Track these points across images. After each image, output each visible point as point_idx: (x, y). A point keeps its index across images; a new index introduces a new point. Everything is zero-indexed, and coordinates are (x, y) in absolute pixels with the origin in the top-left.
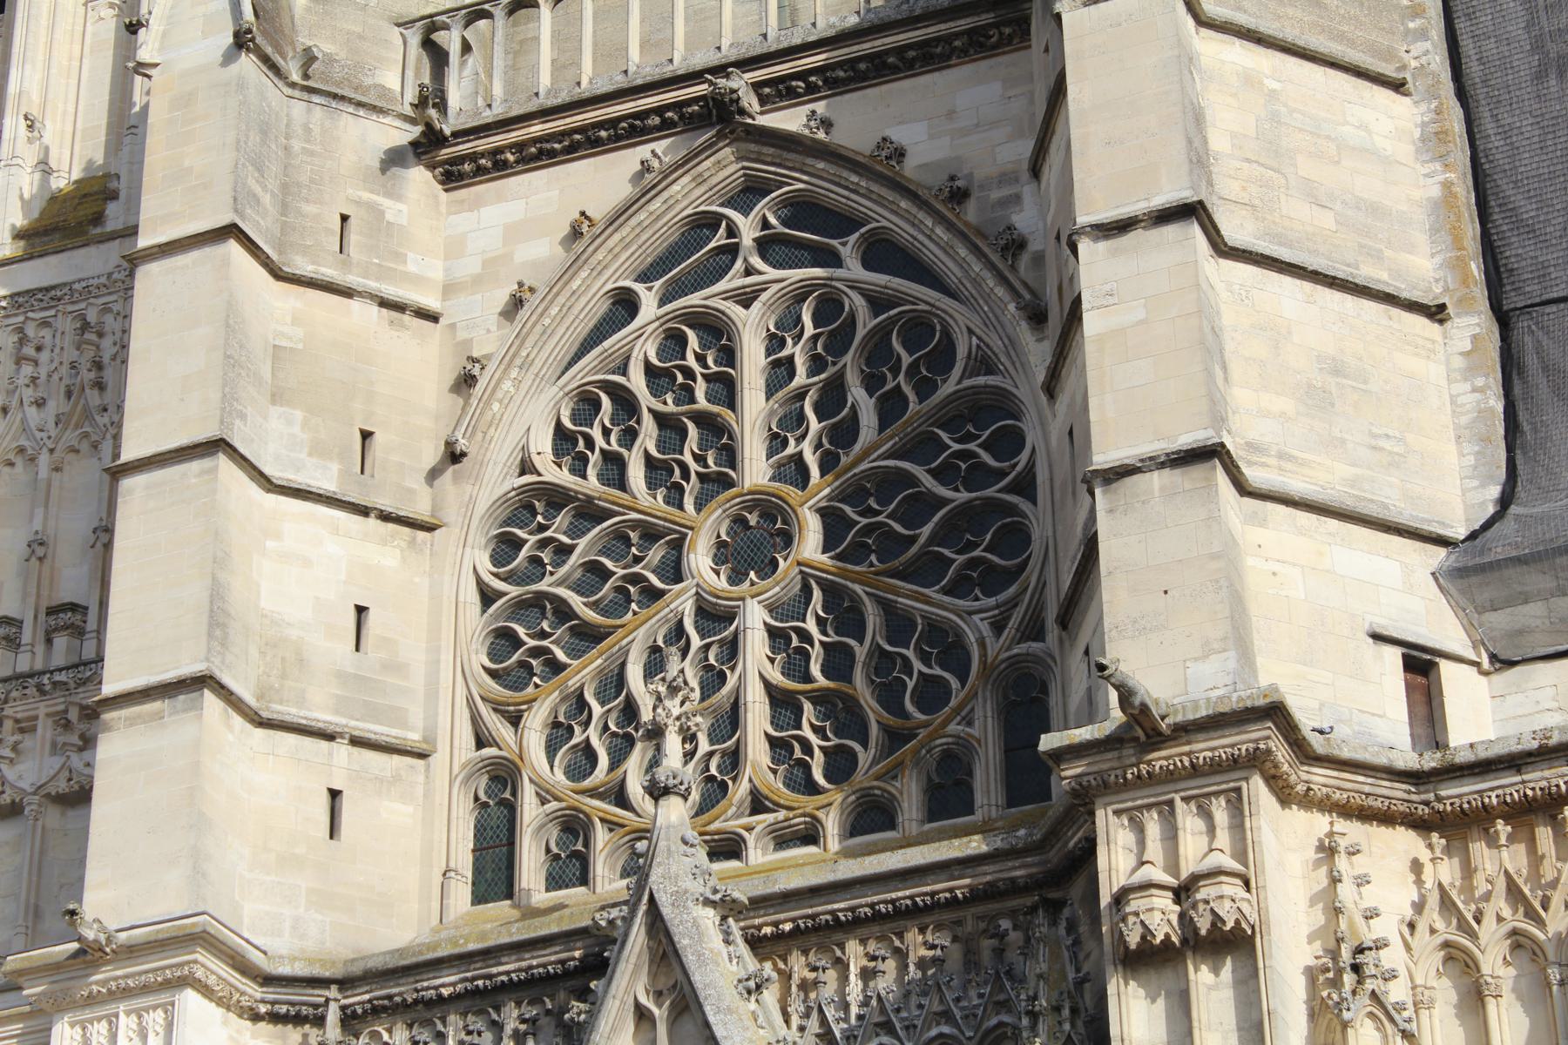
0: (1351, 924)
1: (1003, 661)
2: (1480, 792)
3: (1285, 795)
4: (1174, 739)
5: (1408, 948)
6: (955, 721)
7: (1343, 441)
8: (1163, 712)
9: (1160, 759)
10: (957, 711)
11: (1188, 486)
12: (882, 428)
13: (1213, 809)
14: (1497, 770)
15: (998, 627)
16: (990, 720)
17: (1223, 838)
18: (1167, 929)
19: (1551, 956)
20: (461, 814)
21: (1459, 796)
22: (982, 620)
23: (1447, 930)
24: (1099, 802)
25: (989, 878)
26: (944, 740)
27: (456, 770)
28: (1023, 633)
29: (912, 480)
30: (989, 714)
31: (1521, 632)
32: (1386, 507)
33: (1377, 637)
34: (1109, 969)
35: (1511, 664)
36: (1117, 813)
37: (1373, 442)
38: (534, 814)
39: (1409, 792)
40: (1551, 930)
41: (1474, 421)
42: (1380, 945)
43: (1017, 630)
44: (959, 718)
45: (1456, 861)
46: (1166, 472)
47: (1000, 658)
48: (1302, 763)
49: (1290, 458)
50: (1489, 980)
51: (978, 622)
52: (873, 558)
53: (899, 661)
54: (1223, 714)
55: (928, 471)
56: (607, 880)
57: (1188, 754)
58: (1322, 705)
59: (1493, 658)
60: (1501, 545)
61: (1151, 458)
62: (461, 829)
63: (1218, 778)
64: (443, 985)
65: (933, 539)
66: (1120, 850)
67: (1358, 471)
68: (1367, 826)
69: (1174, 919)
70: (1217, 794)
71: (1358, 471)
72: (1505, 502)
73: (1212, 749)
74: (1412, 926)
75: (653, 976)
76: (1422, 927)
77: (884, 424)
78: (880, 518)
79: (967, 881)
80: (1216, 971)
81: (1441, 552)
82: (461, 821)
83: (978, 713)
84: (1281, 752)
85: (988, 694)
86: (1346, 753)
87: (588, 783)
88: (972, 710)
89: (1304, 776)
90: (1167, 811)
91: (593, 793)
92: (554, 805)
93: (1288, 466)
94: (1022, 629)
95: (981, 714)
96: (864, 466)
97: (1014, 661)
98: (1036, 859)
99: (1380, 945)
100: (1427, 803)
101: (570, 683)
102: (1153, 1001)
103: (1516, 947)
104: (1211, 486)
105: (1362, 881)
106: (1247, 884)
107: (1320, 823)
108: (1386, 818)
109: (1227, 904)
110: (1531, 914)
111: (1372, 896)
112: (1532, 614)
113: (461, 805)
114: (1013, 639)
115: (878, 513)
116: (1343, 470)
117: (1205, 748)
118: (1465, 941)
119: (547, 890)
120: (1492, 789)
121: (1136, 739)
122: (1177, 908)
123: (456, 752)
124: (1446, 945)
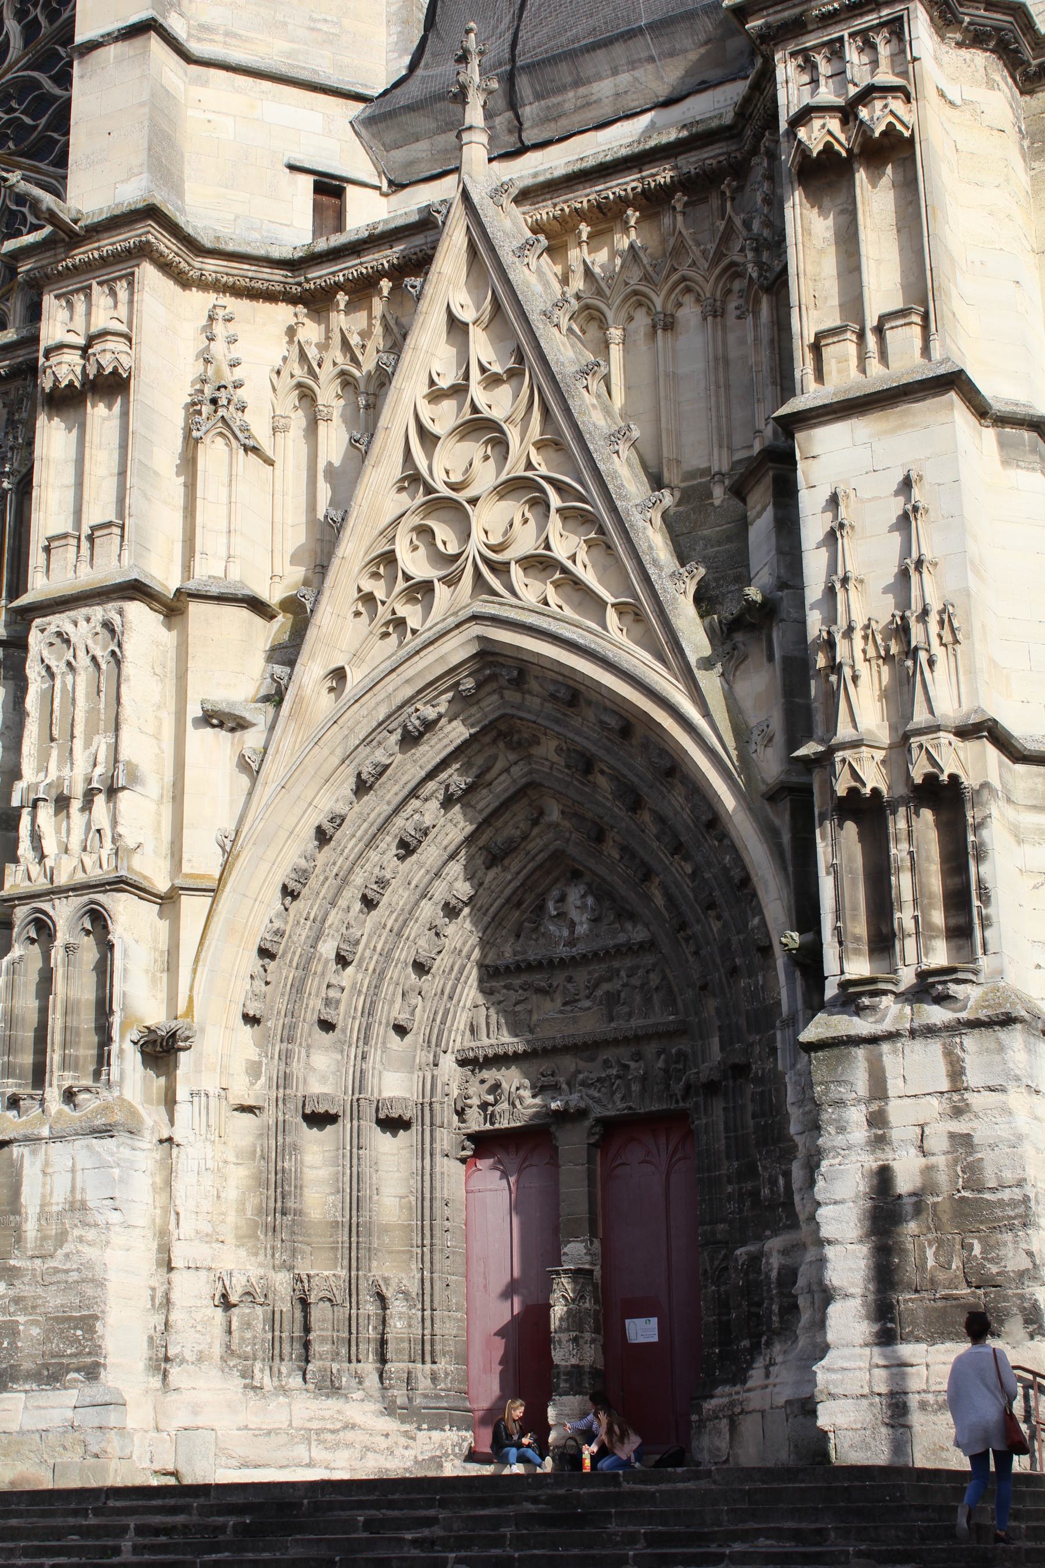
0: (218, 372)
2: (333, 273)
3: (184, 281)
4: (90, 238)
5: (274, 389)
7: (285, 24)
8: (74, 215)
9: (81, 255)
11: (131, 53)
12: (26, 45)
13: (117, 289)
14: (345, 256)
17: (123, 311)
18: (71, 377)
19: (362, 388)
21: (320, 277)
23: (300, 373)
24: (46, 290)
25: (20, 359)
29: (36, 84)
31: (410, 164)
32: (316, 72)
33: (292, 168)
34: (39, 409)
35: (403, 186)
36: (57, 297)
37: (312, 25)
39: (286, 277)
40: (365, 370)
41: (400, 8)
42: (238, 385)
45: (323, 326)
46: (120, 44)
48: (197, 256)
49: (235, 36)
50: (321, 408)
52: (11, 144)
53: (20, 216)
54: (116, 217)
55: (50, 77)
57: (98, 249)
58: (237, 217)
59: (391, 183)
60: (402, 98)
61: (109, 34)
63: (121, 266)
65: (48, 127)
66: (58, 324)
67: (296, 46)
68: (254, 303)
69: (78, 370)
70: (120, 278)
71: (296, 46)
72: (413, 67)
73: (112, 244)
74: (278, 373)
76: (285, 374)
77: (26, 44)
78: (16, 114)
79: (7, 363)
80: (110, 407)
81: (361, 106)
84: (166, 245)
86: (231, 247)
89: (198, 265)
90: (87, 290)
93: (234, 42)
96: (9, 77)
99: (238, 385)
100: (299, 284)
102: (70, 431)
103: (345, 384)
104: (146, 50)
105: (232, 341)
106: (130, 340)
107: (211, 298)
108: (269, 296)
109: (109, 356)
110: (354, 360)
111: (237, 351)
112: (421, 149)
115: (15, 110)
116: (285, 46)
117: (109, 244)
118: (311, 383)
120: (341, 270)
121: (63, 240)
122: (82, 362)
124: (299, 385)
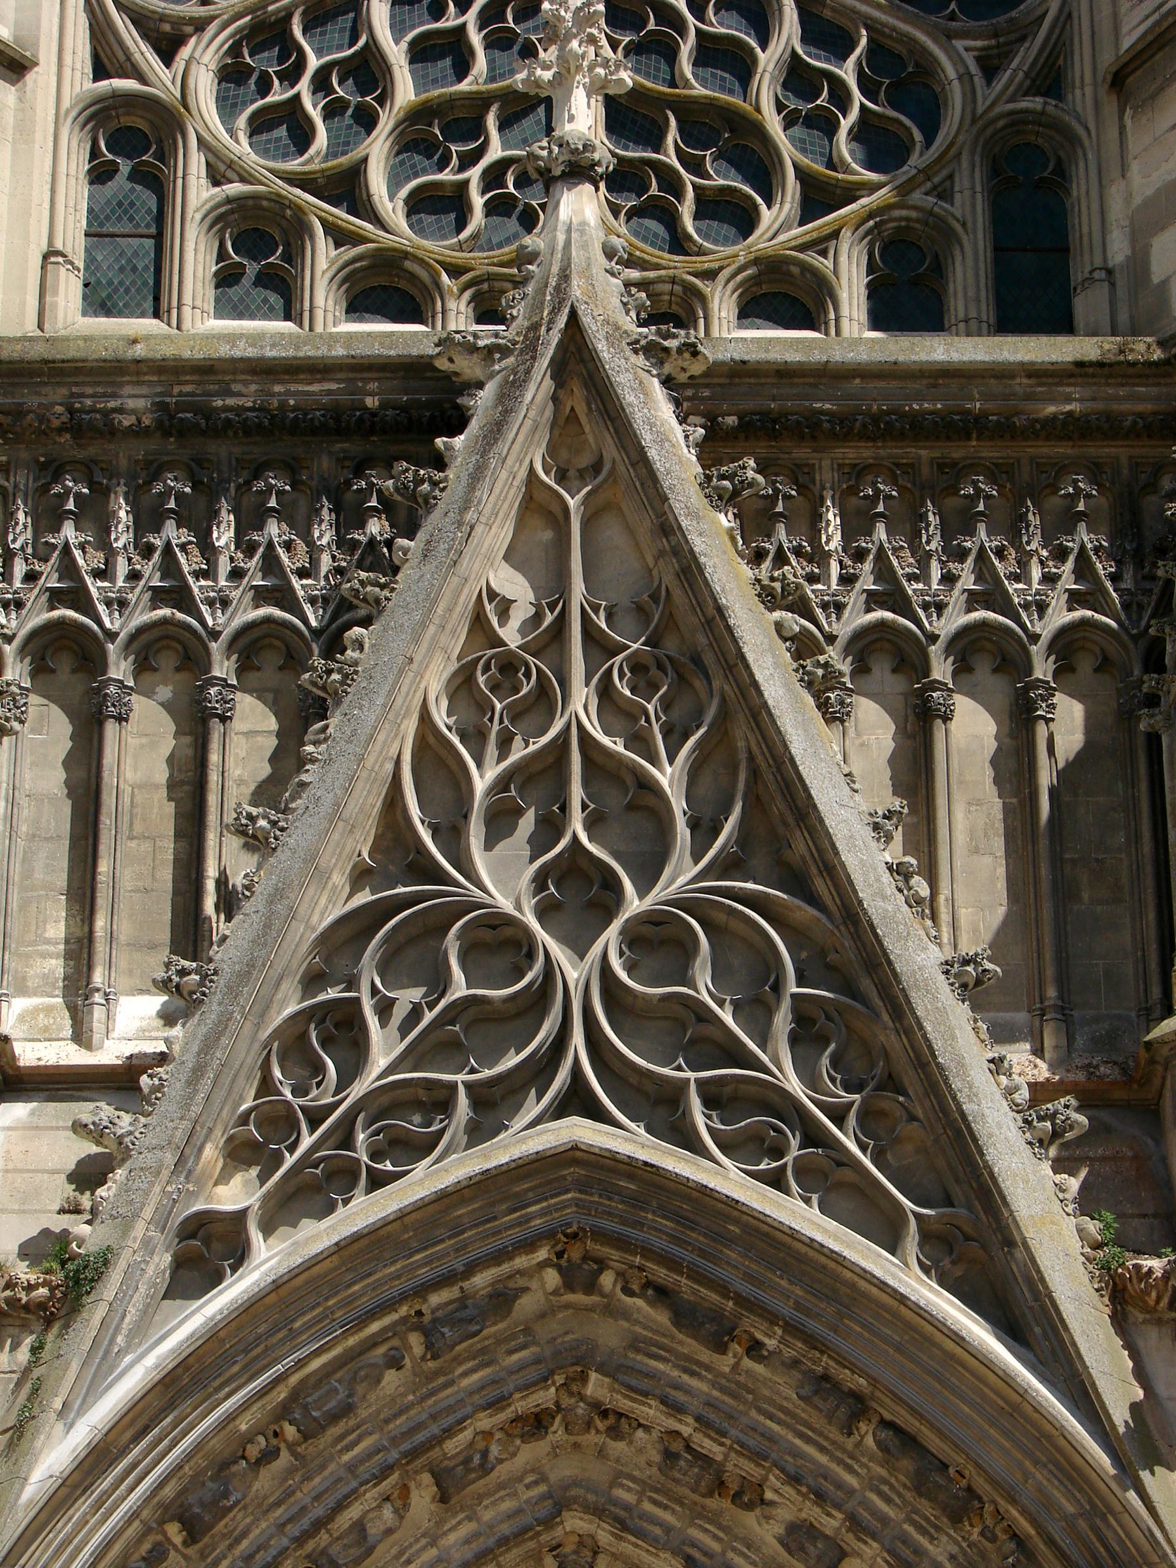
1: (1002, 116)
6: (923, 189)
10: (926, 173)
15: (990, 67)
16: (979, 196)
20: (73, 172)
22: (967, 49)
26: (904, 213)
27: (66, 103)
28: (1034, 81)
30: (978, 188)
38: (205, 195)
43: (1027, 74)
44: (929, 185)
47: (998, 110)
51: (964, 54)
56: (330, 317)
62: (72, 193)
64: (120, 410)
75: (552, 450)
82: (73, 181)
83: (962, 182)
85: (977, 158)
87: (294, 165)
88: (951, 177)
91: (303, 181)
92: (235, 188)
94: (1033, 75)
95: (966, 183)
97: (1018, 120)
98: (1154, 391)
101: (270, 8)
113: (74, 156)
114: (1021, 84)
119: (219, 315)
123: (67, 72)
